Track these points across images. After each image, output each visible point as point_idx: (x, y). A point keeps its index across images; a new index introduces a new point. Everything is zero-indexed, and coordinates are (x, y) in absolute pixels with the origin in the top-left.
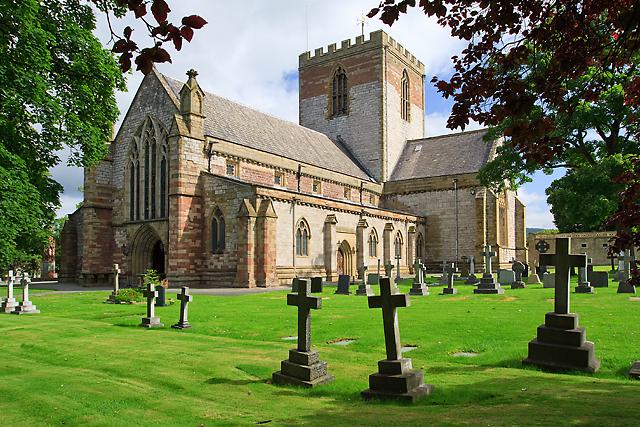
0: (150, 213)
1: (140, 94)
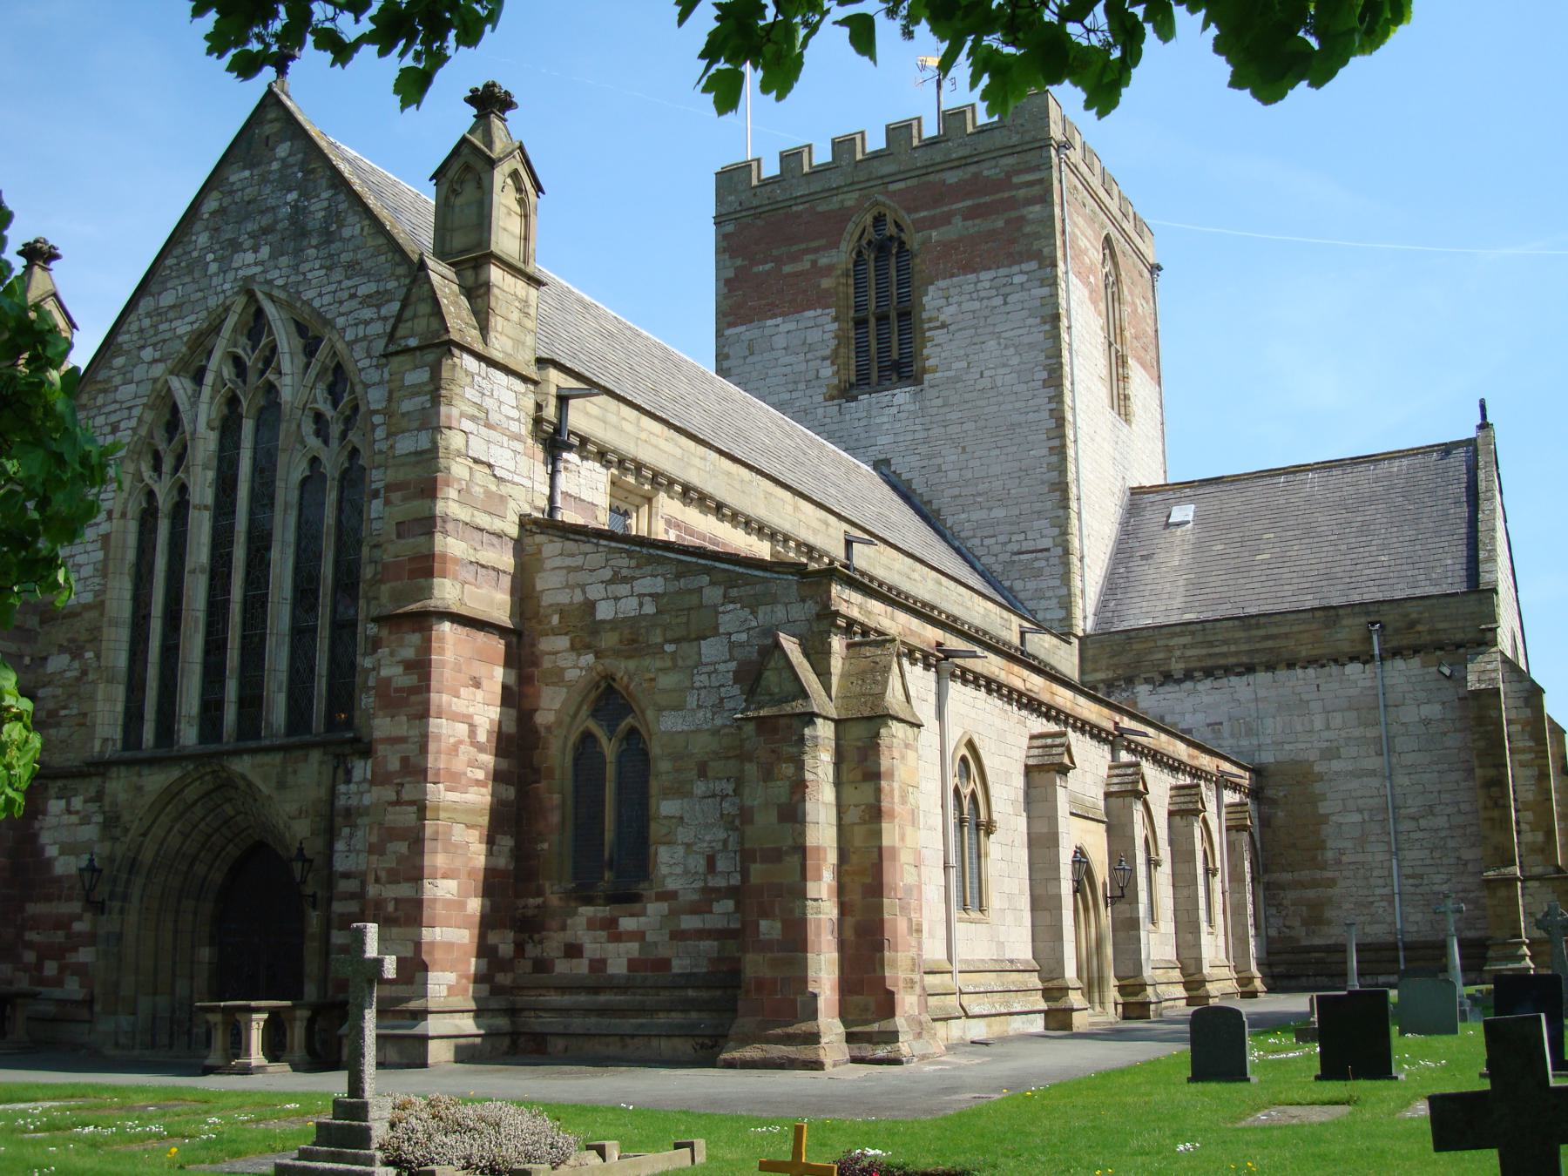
0: (230, 714)
1: (211, 205)
